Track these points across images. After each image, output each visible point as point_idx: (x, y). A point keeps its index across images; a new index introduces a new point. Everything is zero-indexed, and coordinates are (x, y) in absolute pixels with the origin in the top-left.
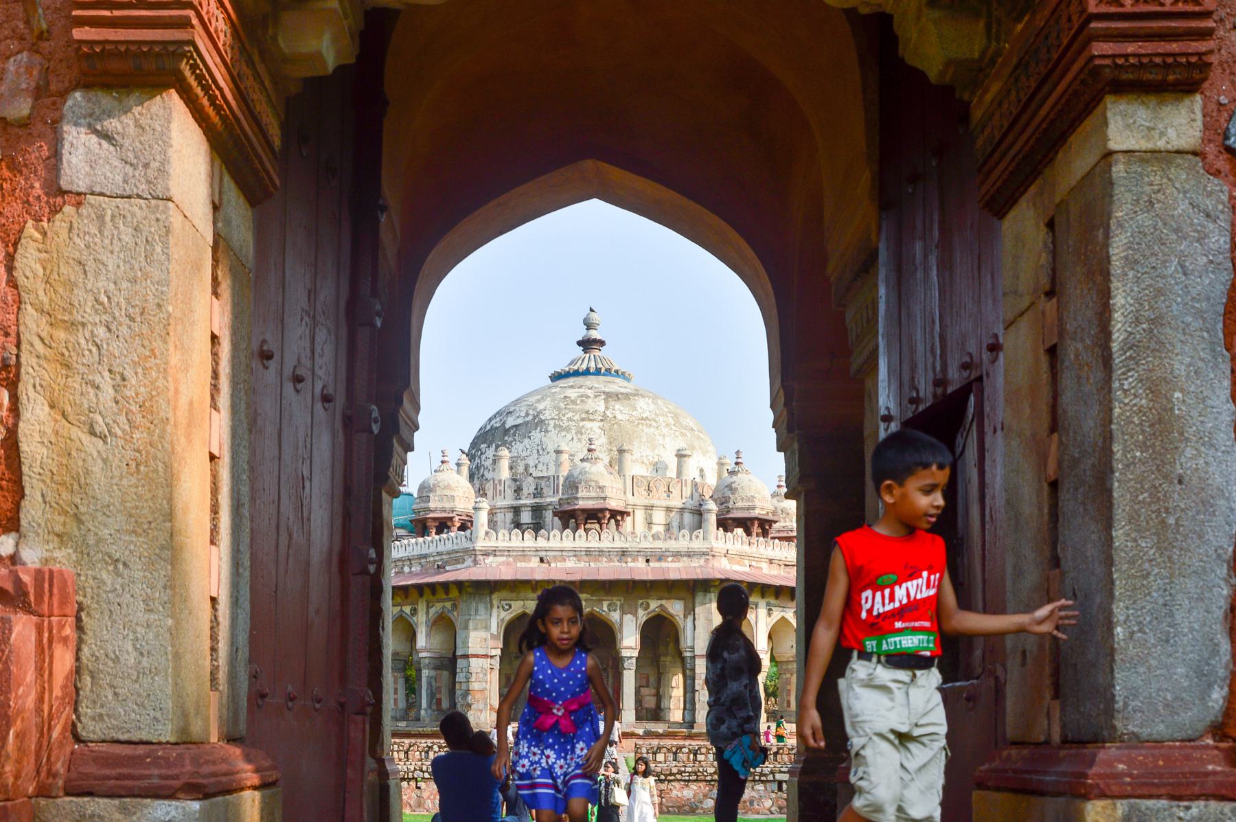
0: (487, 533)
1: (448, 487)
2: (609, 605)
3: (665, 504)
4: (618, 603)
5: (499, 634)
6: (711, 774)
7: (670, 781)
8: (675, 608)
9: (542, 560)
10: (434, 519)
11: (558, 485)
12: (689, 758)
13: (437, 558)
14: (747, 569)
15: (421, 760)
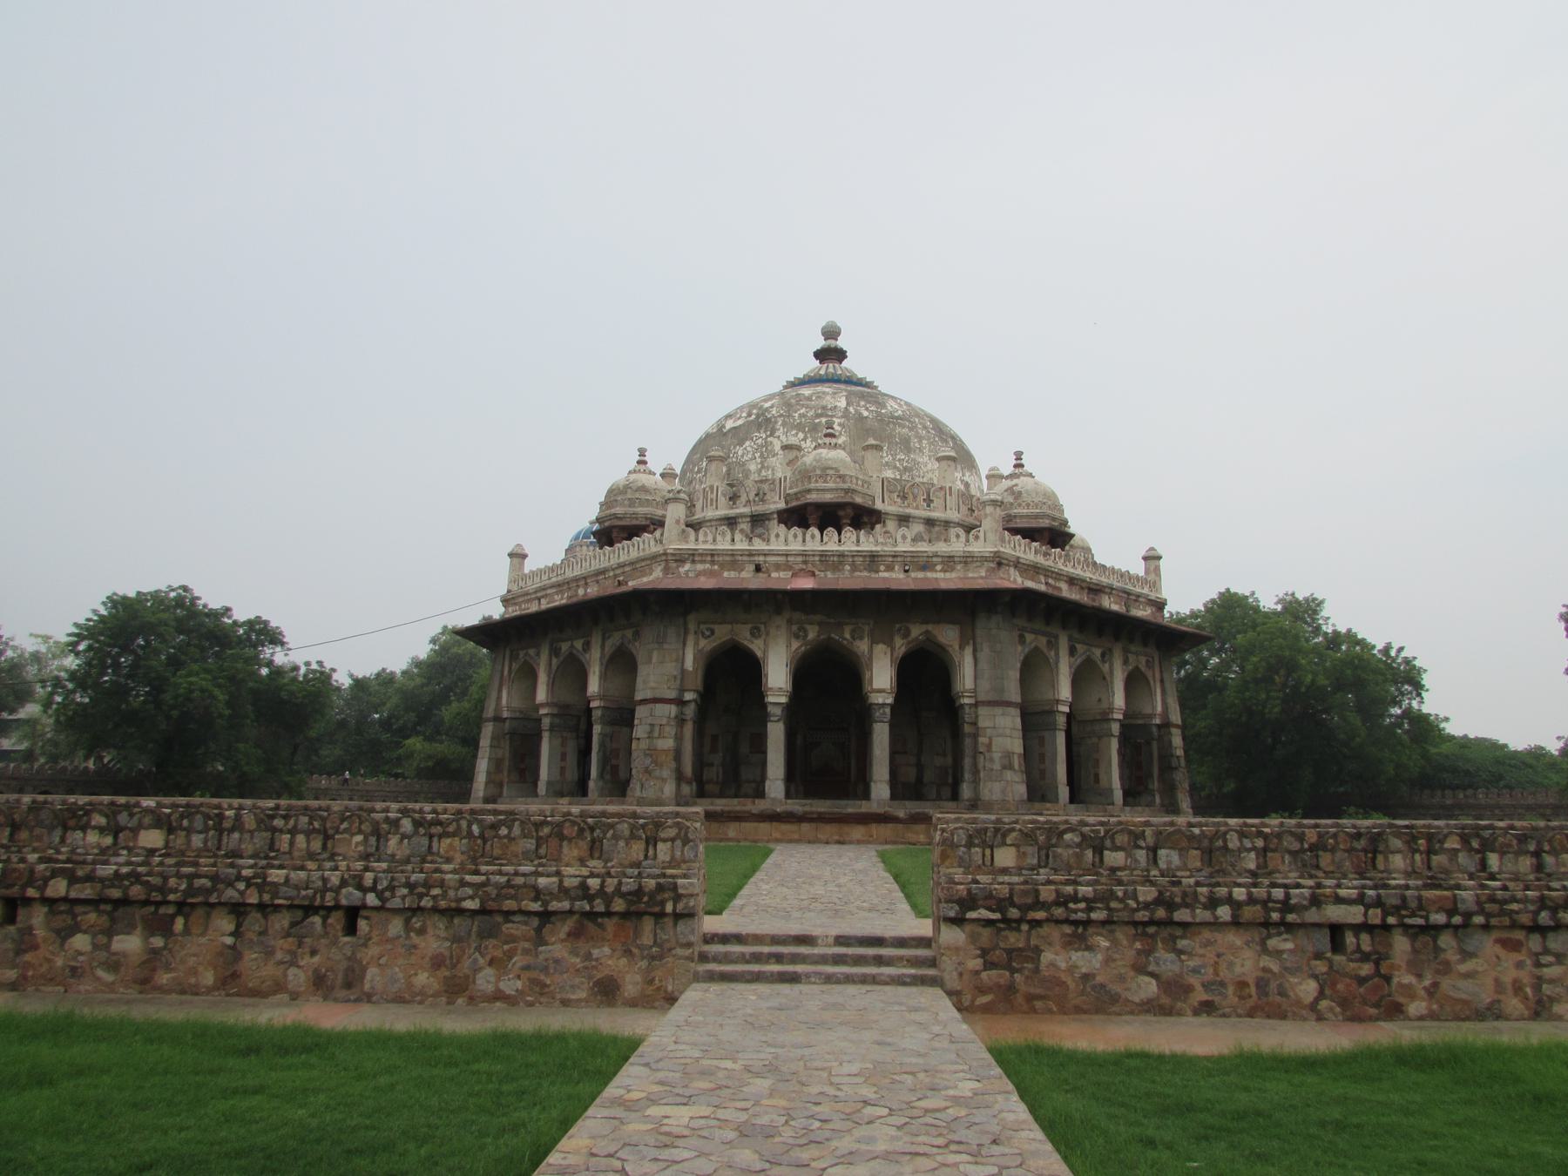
0: (683, 531)
1: (643, 489)
2: (853, 632)
3: (924, 513)
4: (866, 628)
5: (695, 669)
6: (1147, 906)
7: (1036, 924)
8: (947, 635)
9: (758, 569)
10: (623, 528)
11: (785, 488)
12: (1079, 857)
13: (618, 572)
14: (1042, 588)
15: (366, 857)
